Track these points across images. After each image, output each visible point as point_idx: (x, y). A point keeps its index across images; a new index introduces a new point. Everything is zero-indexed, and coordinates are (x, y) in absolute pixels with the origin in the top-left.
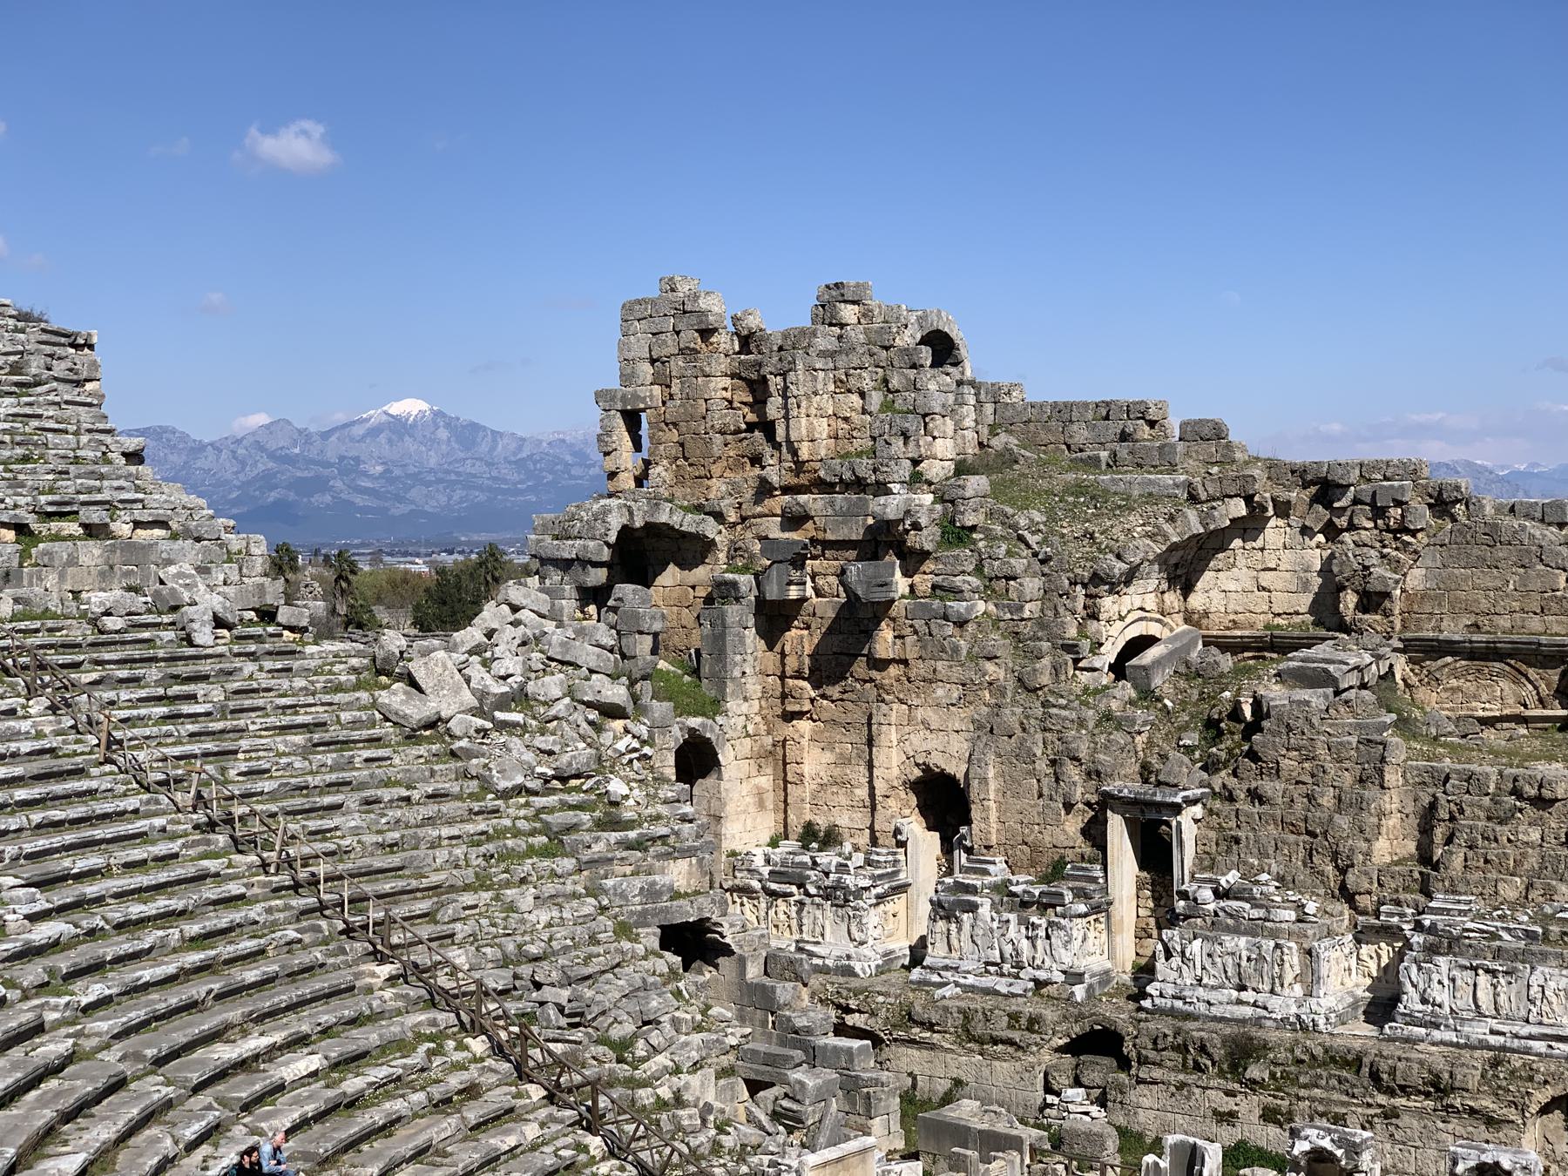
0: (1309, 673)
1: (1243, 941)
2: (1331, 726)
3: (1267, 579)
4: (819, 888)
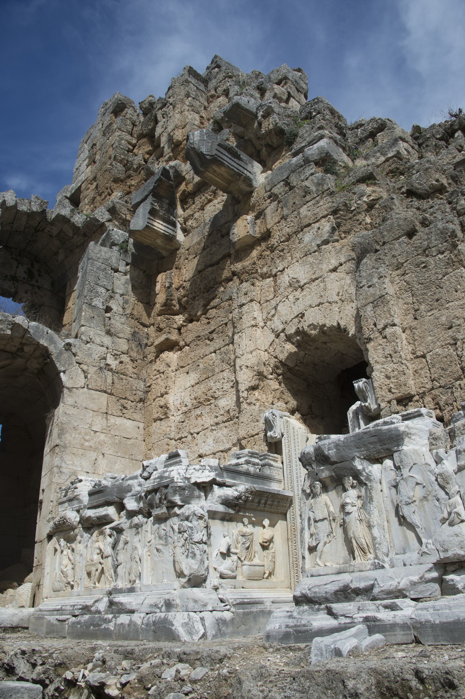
4: (139, 499)
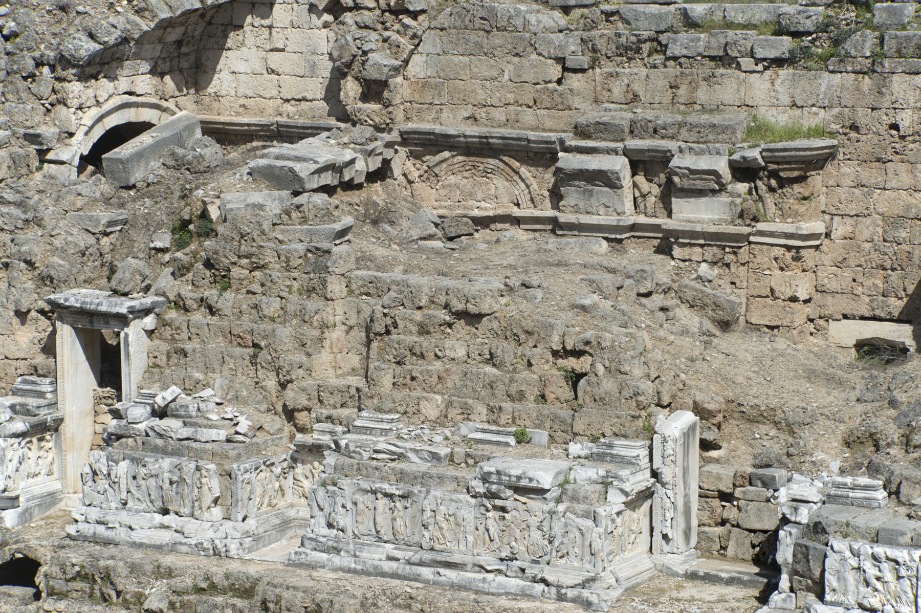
0: (277, 172)
1: (166, 463)
2: (283, 232)
3: (275, 60)
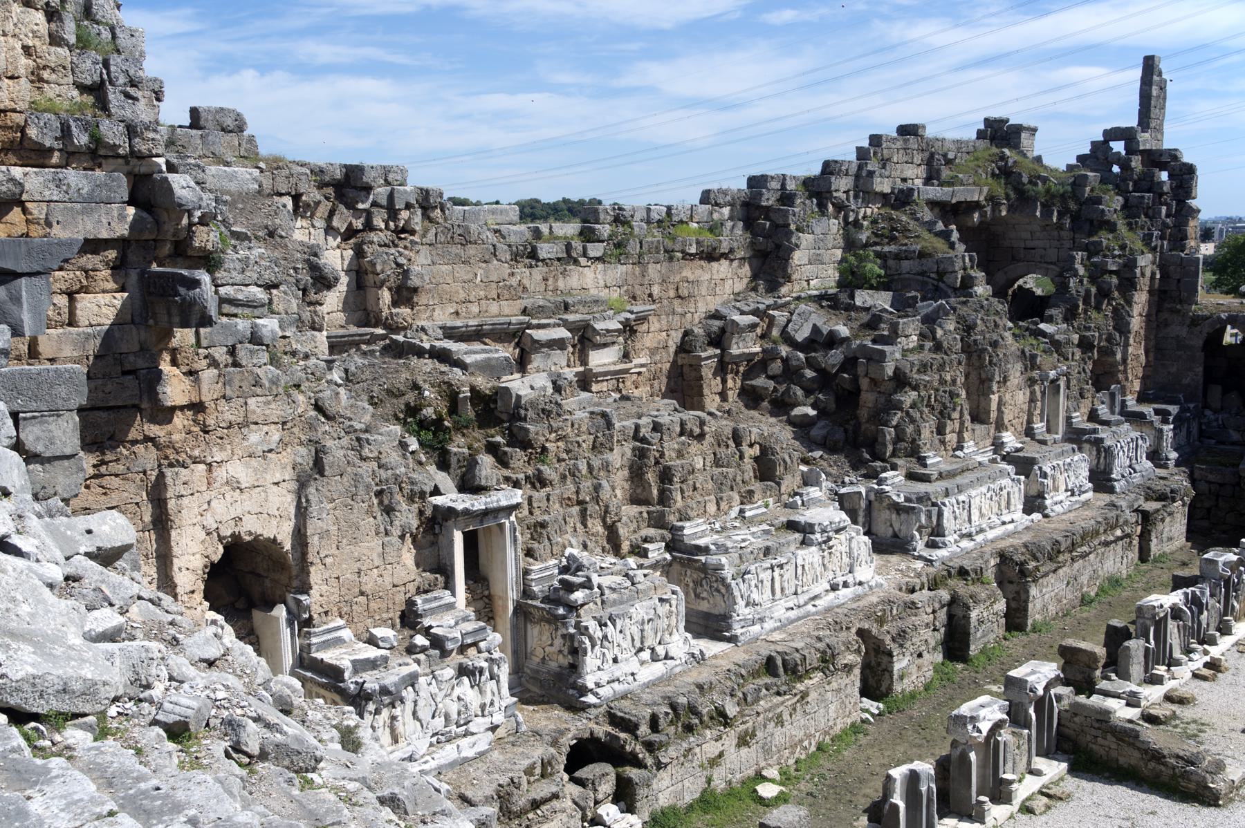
0: (493, 362)
